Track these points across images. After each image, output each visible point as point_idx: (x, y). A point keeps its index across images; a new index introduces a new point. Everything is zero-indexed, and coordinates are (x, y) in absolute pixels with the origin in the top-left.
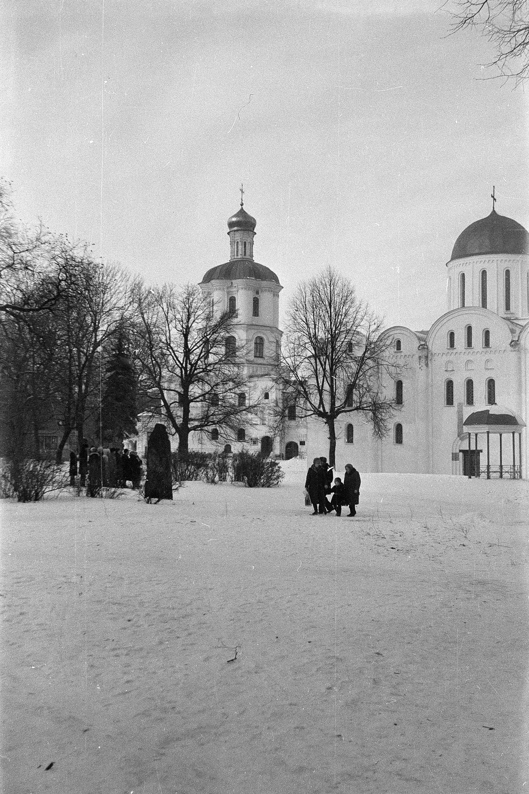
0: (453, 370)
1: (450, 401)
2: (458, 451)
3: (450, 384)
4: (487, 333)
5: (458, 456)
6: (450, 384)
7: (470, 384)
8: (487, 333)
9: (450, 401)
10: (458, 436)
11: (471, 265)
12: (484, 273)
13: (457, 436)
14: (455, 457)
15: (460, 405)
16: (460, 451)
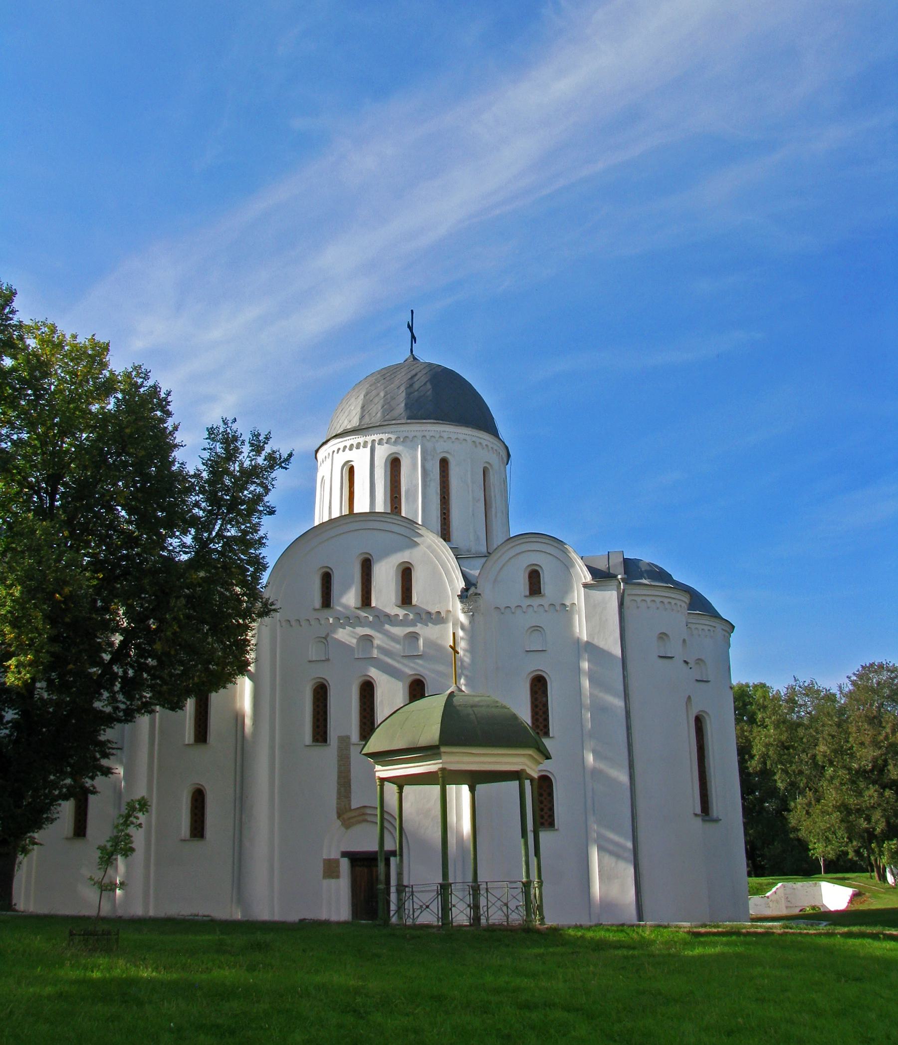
0: (328, 660)
1: (320, 734)
2: (338, 856)
3: (321, 693)
4: (406, 574)
5: (338, 865)
6: (321, 693)
7: (367, 690)
8: (406, 574)
9: (320, 734)
10: (339, 817)
11: (368, 450)
12: (394, 464)
13: (335, 816)
14: (331, 869)
15: (345, 741)
16: (345, 854)
